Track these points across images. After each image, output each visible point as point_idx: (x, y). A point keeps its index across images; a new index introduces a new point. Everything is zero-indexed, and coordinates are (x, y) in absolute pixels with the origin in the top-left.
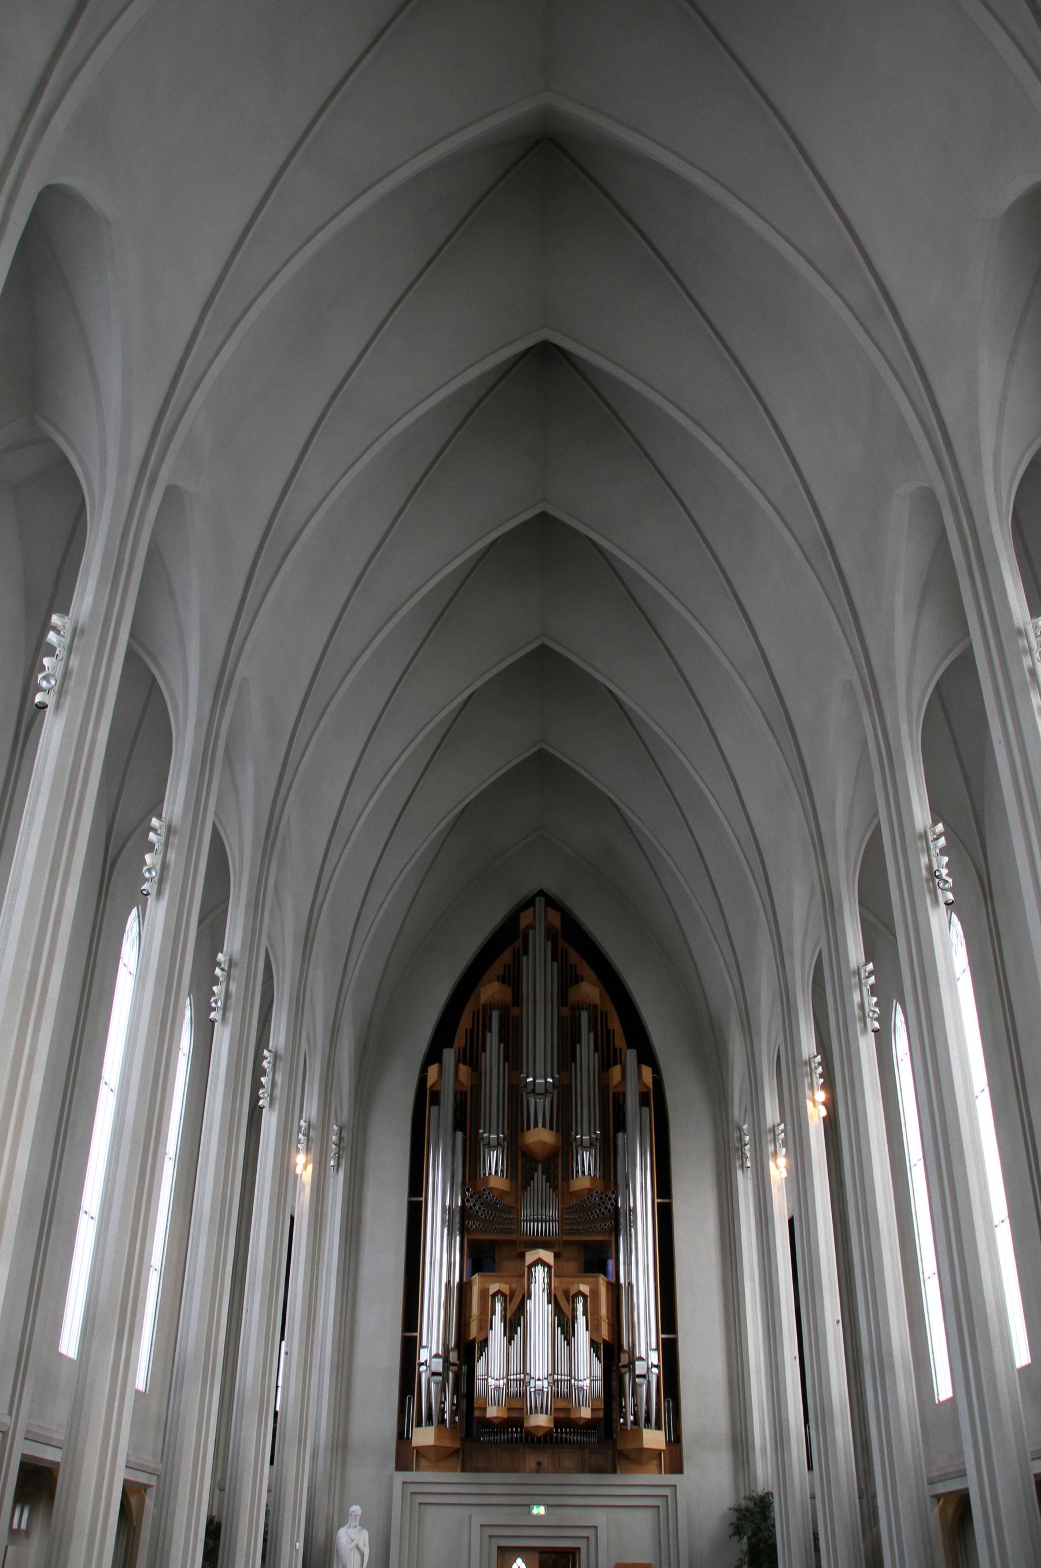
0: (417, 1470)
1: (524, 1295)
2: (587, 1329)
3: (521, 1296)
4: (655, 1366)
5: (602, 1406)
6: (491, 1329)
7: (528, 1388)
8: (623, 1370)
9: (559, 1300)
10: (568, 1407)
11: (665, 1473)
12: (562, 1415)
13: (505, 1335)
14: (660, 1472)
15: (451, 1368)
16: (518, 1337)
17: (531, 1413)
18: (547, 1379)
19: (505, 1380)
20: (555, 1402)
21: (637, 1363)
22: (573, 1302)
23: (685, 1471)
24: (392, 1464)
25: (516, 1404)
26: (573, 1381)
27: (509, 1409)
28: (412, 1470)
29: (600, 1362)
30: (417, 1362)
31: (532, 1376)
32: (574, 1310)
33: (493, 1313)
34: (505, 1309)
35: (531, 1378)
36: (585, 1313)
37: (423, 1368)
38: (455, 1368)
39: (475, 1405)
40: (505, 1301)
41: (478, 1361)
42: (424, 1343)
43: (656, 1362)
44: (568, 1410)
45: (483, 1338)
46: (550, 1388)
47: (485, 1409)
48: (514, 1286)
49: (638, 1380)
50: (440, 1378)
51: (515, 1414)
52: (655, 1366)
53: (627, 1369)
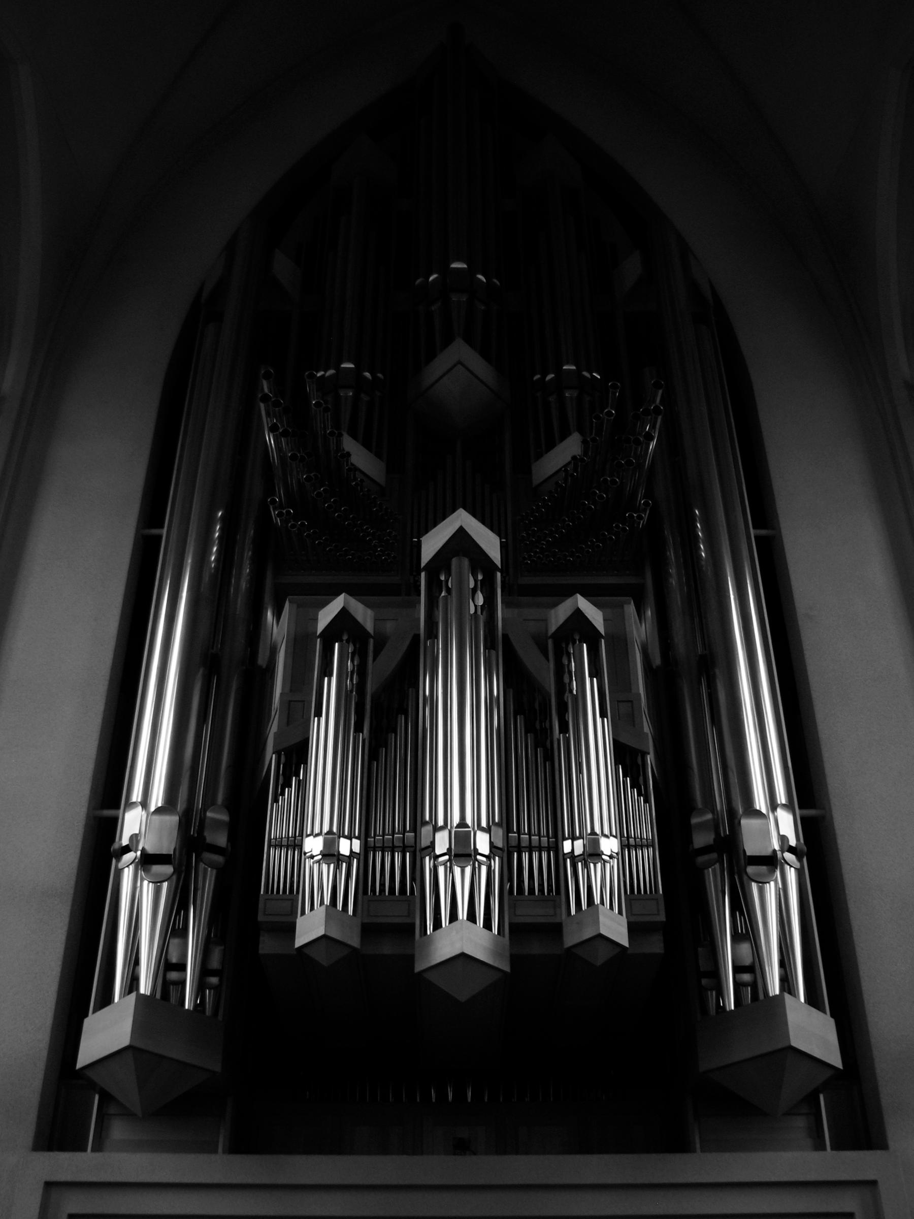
0: (97, 1148)
1: (416, 637)
2: (603, 715)
3: (407, 642)
4: (791, 850)
5: (662, 918)
6: (318, 714)
7: (428, 863)
8: (701, 859)
9: (521, 652)
10: (557, 920)
11: (832, 1149)
12: (536, 948)
13: (359, 728)
14: (823, 1148)
15: (207, 856)
16: (397, 741)
17: (437, 925)
18: (488, 830)
19: (357, 845)
20: (513, 907)
21: (747, 824)
22: (561, 654)
23: (891, 1143)
24: (27, 1131)
25: (392, 914)
26: (567, 846)
27: (369, 930)
28: (85, 1150)
29: (647, 801)
30: (116, 846)
31: (441, 823)
32: (561, 671)
33: (326, 671)
34: (362, 671)
35: (436, 829)
36: (596, 672)
37: (129, 857)
38: (219, 859)
39: (261, 918)
40: (361, 653)
41: (276, 800)
42: (137, 795)
43: (793, 842)
44: (555, 930)
45: (297, 739)
46: (496, 864)
47: (290, 929)
48: (389, 627)
49: (751, 870)
50: (168, 869)
51: (388, 948)
52: (791, 850)
53: (714, 856)
